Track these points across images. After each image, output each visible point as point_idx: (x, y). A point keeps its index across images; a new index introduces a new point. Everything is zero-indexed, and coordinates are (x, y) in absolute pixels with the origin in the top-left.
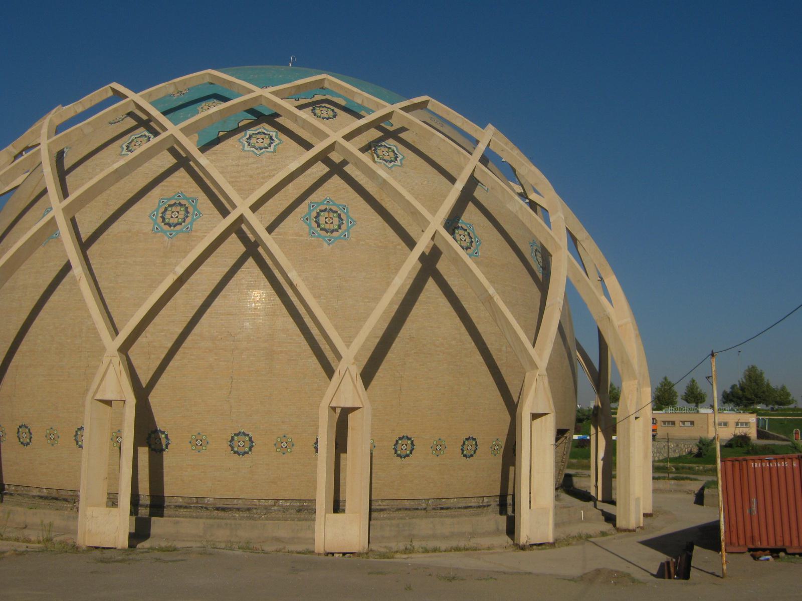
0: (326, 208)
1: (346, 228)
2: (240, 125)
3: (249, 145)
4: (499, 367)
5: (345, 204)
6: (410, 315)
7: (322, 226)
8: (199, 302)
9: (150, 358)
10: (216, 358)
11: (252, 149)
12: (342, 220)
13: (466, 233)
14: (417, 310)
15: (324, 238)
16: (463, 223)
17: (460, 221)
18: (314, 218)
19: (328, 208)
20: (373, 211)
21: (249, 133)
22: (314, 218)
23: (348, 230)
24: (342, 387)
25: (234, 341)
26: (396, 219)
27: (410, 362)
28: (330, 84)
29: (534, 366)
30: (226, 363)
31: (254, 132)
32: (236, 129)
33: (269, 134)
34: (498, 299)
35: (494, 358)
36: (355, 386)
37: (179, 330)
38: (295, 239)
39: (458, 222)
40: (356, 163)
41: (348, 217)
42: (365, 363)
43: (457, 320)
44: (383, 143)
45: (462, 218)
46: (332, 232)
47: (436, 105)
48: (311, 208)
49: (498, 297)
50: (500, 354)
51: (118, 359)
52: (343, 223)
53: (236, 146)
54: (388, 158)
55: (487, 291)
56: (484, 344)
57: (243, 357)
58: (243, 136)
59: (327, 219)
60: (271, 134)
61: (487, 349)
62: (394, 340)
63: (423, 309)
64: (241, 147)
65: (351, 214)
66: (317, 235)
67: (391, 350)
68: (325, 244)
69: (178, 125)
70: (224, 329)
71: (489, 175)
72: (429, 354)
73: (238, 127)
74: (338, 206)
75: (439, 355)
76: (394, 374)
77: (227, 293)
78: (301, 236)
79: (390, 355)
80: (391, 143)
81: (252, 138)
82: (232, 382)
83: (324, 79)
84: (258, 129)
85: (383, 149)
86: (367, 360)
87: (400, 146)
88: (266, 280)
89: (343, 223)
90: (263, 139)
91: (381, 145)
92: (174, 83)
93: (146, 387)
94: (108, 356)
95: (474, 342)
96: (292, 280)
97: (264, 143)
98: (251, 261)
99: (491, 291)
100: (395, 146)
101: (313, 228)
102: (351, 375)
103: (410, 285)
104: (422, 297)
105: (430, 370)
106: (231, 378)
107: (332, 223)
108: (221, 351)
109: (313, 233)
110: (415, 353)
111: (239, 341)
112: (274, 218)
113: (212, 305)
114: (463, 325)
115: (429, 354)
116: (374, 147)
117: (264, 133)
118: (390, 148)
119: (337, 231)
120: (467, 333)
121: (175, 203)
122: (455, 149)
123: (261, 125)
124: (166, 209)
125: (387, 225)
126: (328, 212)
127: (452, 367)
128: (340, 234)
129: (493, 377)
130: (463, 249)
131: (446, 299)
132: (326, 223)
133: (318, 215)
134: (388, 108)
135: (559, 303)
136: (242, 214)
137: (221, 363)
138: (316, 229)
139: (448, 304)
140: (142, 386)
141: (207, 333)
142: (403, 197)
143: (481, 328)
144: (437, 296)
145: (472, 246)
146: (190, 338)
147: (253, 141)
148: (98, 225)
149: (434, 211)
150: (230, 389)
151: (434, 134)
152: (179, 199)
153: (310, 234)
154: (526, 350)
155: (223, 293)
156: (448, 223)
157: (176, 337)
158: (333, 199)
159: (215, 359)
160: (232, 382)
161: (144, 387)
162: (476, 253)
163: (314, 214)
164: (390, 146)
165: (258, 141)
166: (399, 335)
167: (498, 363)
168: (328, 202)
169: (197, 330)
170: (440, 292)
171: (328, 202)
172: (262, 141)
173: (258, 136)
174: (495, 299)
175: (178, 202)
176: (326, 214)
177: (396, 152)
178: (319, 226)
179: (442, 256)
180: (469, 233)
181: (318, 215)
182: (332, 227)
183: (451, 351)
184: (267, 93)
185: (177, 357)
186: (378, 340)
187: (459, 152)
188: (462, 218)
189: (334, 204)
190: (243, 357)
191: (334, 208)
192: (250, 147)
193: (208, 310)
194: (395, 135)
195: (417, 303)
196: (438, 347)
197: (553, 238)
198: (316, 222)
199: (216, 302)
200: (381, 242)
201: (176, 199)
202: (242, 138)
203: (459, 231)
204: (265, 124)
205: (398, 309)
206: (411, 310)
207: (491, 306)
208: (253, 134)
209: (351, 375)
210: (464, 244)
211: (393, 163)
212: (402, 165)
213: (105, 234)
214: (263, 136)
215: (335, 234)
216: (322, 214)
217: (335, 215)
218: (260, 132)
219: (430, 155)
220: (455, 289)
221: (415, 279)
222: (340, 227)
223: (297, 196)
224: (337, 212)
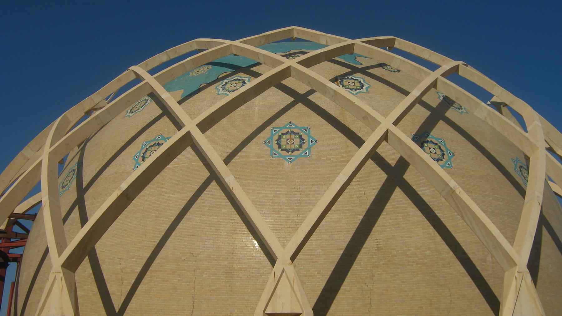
0: (288, 132)
1: (307, 147)
2: (219, 77)
3: (223, 90)
4: (485, 278)
5: (307, 126)
6: (376, 225)
7: (284, 147)
8: (166, 227)
9: (122, 284)
10: (180, 279)
11: (225, 92)
12: (303, 140)
13: (437, 147)
14: (383, 220)
15: (284, 157)
16: (433, 137)
17: (430, 136)
18: (276, 140)
19: (290, 131)
20: (335, 130)
21: (225, 81)
22: (276, 140)
23: (309, 148)
24: (278, 291)
25: (196, 261)
26: (360, 136)
27: (379, 274)
28: (298, 33)
29: (513, 263)
30: (188, 283)
31: (230, 80)
32: (216, 80)
33: (243, 80)
34: (460, 191)
35: (478, 268)
36: (293, 289)
37: (147, 255)
38: (257, 160)
39: (427, 137)
40: (309, 83)
41: (309, 137)
42: (329, 276)
43: (431, 229)
44: (350, 77)
45: (432, 133)
46: (293, 151)
47: (401, 43)
48: (274, 133)
49: (460, 189)
50: (485, 264)
51: (62, 274)
52: (304, 143)
53: (213, 92)
54: (355, 87)
55: (447, 184)
56: (464, 253)
57: (204, 276)
58: (219, 85)
59: (288, 141)
60: (244, 79)
61: (469, 259)
62: (358, 251)
63: (390, 219)
64: (216, 92)
65: (312, 134)
66: (278, 155)
67: (356, 261)
68: (286, 163)
69: (153, 76)
70: (187, 250)
71: (451, 85)
72: (400, 265)
73: (218, 79)
74: (300, 129)
75: (412, 265)
76: (362, 287)
77: (191, 216)
78: (263, 157)
79: (355, 267)
80: (359, 76)
81: (227, 85)
82: (194, 302)
83: (293, 29)
84: (236, 77)
85: (349, 80)
86: (330, 273)
87: (367, 78)
88: (227, 200)
89: (304, 143)
90: (237, 84)
91: (348, 78)
92: (166, 52)
93: (118, 312)
94: (53, 273)
95: (453, 251)
96: (229, 184)
97: (237, 86)
98: (214, 184)
99: (453, 184)
100: (362, 78)
101: (274, 150)
102: (287, 277)
103: (375, 196)
104: (389, 207)
105: (403, 282)
106: (193, 298)
107: (293, 143)
108: (183, 271)
109: (274, 154)
110: (384, 264)
111: (200, 261)
112: (237, 144)
113: (177, 228)
114: (438, 234)
115: (400, 265)
116: (340, 79)
117: (238, 80)
118: (357, 80)
119: (298, 150)
120: (443, 242)
121: (155, 144)
122: (415, 67)
123: (237, 75)
124: (147, 150)
125: (349, 141)
126: (290, 134)
127: (428, 278)
128: (301, 152)
129: (479, 290)
130: (435, 160)
131: (416, 208)
132: (288, 143)
133: (280, 137)
134: (349, 41)
135: (538, 197)
136: (189, 131)
137: (184, 283)
138: (277, 150)
139: (420, 214)
140: (116, 311)
141: (172, 255)
142: (352, 103)
143: (459, 237)
144: (406, 206)
145: (444, 158)
146: (156, 261)
147: (228, 86)
148: (96, 172)
149: (385, 115)
150: (192, 310)
151: (394, 57)
152: (158, 140)
153: (270, 155)
154: (498, 245)
155: (187, 216)
156: (416, 138)
157: (144, 261)
158: (296, 123)
159: (179, 281)
160: (194, 302)
161: (117, 312)
162: (449, 165)
163: (276, 137)
164: (356, 79)
165: (232, 86)
166: (364, 246)
167: (484, 274)
168: (290, 126)
169: (163, 253)
170: (409, 201)
171: (290, 126)
172: (236, 85)
173: (232, 82)
174: (457, 192)
175: (157, 143)
176: (288, 136)
177: (362, 82)
178: (280, 146)
179: (410, 167)
180: (440, 147)
181: (280, 137)
182: (293, 147)
183: (425, 261)
184: (237, 43)
185: (145, 281)
186: (341, 252)
187: (419, 70)
188: (431, 134)
189: (296, 127)
190: (204, 276)
191: (296, 131)
192: (224, 91)
193: (173, 233)
194: (364, 71)
195: (383, 213)
196: (410, 257)
197: (528, 139)
198: (277, 144)
199: (180, 226)
200: (343, 157)
201: (156, 140)
202: (218, 86)
203: (429, 144)
204: (241, 73)
205: (362, 220)
206: (377, 219)
207: (454, 200)
208: (229, 81)
209: (287, 277)
210: (436, 157)
211: (358, 91)
212: (367, 92)
213: (99, 178)
214: (237, 82)
215: (296, 153)
216: (284, 136)
217: (297, 136)
218: (235, 79)
219: (398, 84)
220: (426, 199)
221: (381, 189)
222: (301, 146)
223: (260, 124)
224: (298, 133)
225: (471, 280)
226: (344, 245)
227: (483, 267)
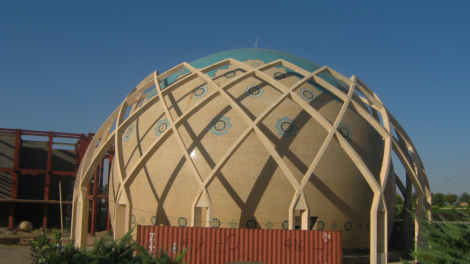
61: (224, 177)
110: (185, 181)
156: (214, 120)
167: (231, 184)
186: (170, 176)
188: (224, 116)
225: (223, 187)
226: (171, 173)
227: (231, 180)
